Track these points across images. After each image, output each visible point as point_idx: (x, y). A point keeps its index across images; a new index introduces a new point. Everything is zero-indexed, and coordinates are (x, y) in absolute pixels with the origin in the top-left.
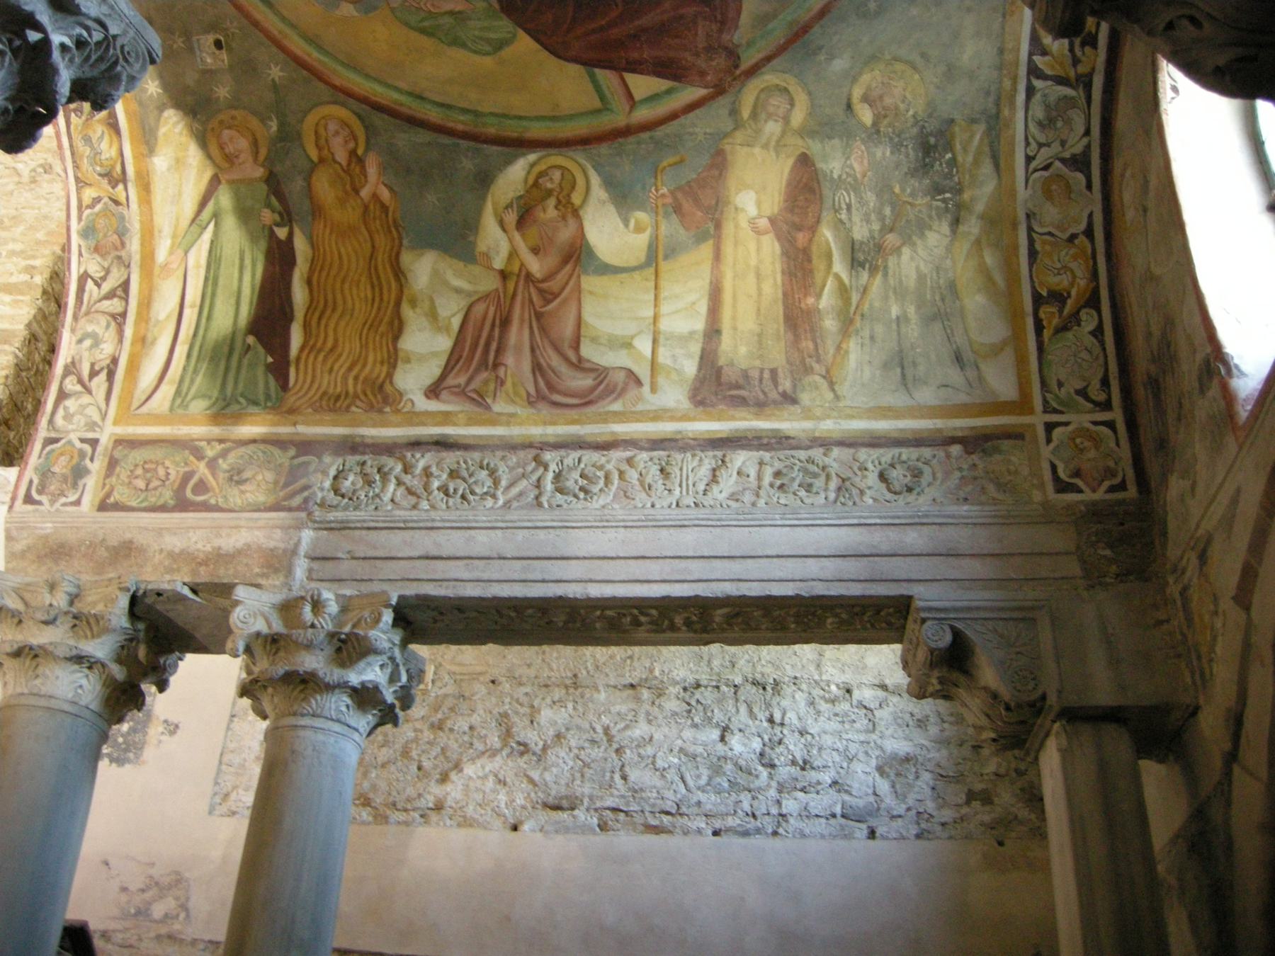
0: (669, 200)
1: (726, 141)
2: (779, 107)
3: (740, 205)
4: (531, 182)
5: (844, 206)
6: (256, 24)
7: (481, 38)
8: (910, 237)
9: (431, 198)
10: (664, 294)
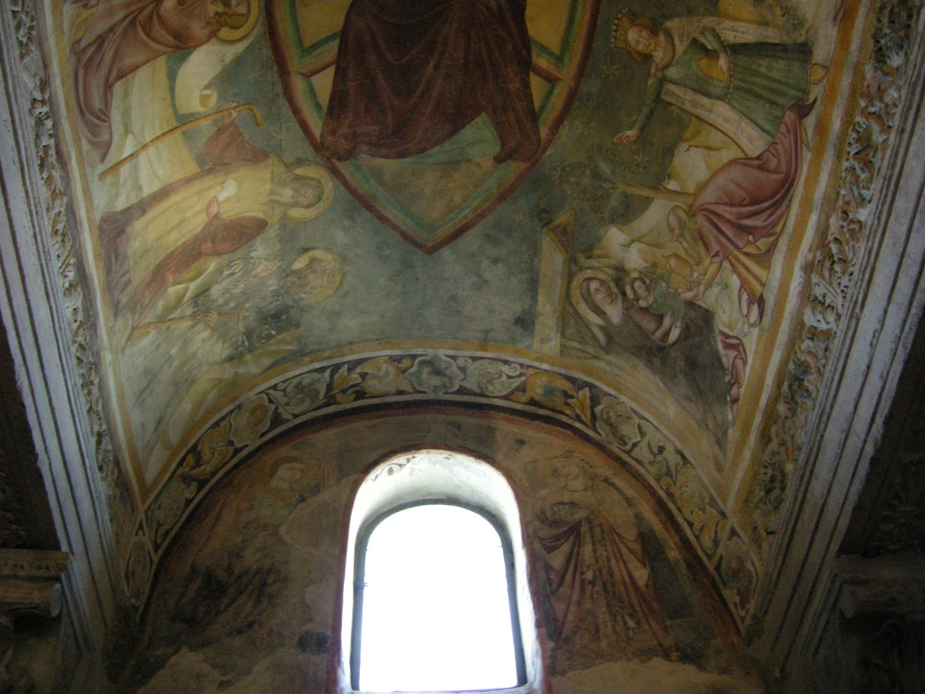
0: (227, 121)
1: (275, 159)
3: (226, 184)
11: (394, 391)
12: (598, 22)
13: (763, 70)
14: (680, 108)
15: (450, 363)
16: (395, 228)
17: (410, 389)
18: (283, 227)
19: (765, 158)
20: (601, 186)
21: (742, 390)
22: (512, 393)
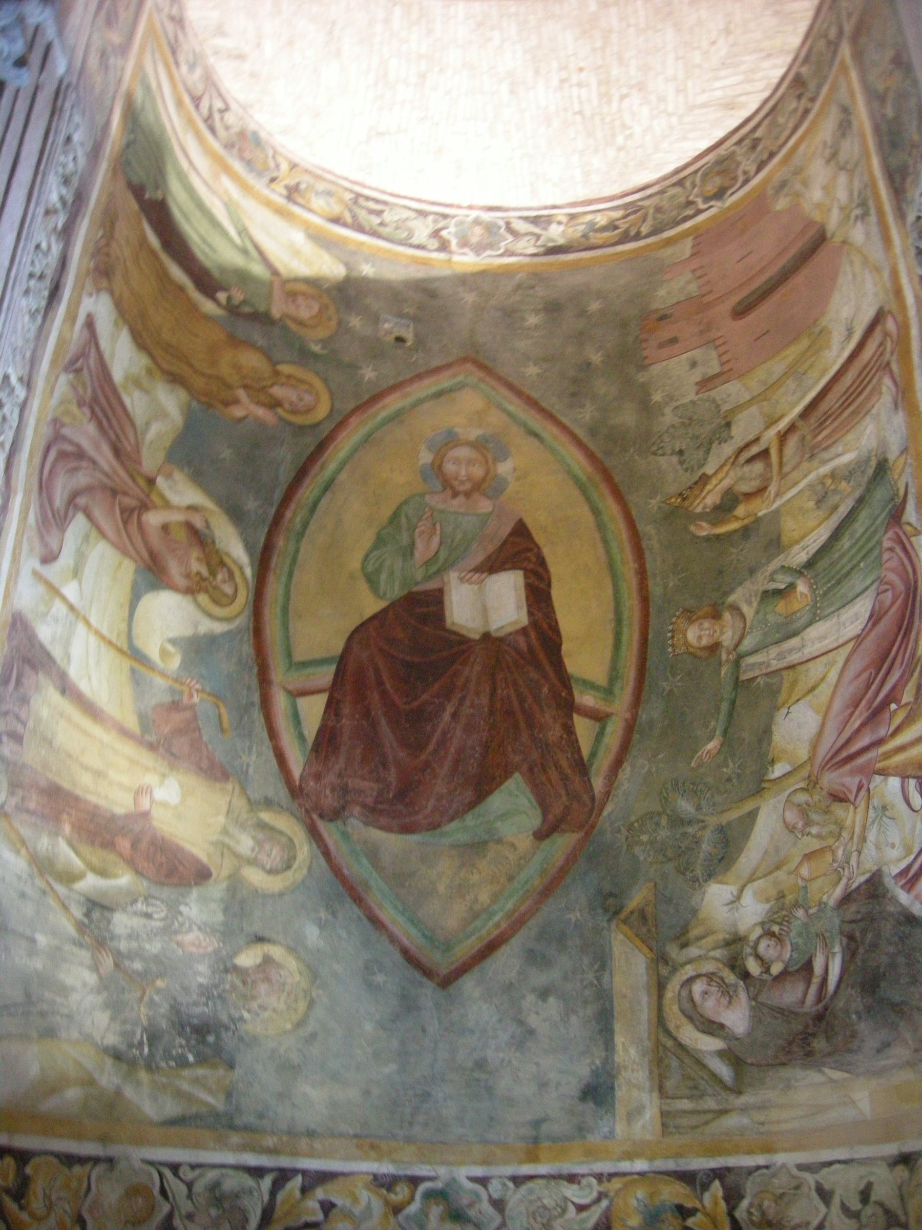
0: (185, 700)
2: (269, 856)
3: (166, 782)
4: (226, 560)
5: (150, 910)
6: (419, 377)
7: (381, 565)
8: (106, 988)
9: (226, 454)
10: (104, 648)
12: (650, 637)
14: (766, 674)
15: (477, 1195)
16: (393, 939)
20: (685, 835)
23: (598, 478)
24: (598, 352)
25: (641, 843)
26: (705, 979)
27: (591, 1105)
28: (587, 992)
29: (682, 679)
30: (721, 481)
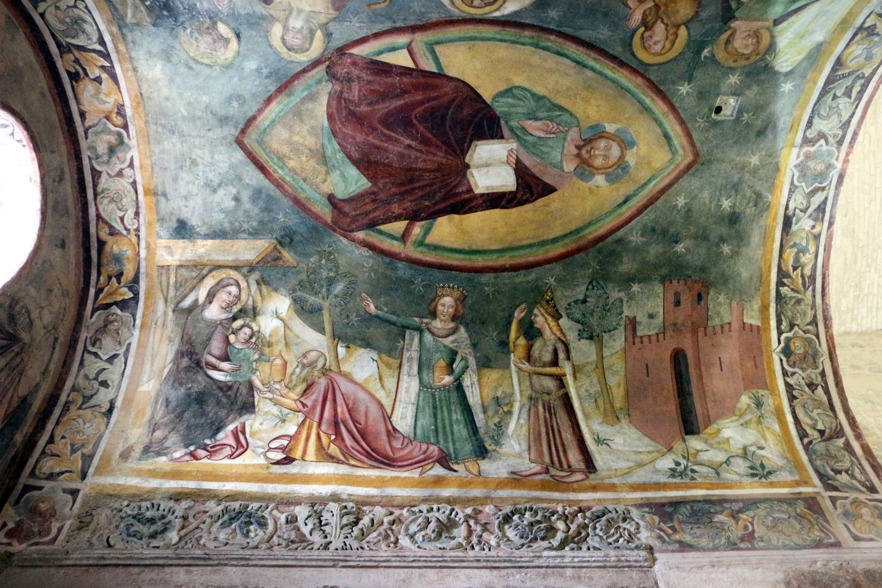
1: (333, 16)
6: (682, 122)
7: (520, 99)
11: (82, 108)
13: (454, 417)
15: (124, 161)
16: (260, 111)
17: (87, 124)
18: (263, 18)
19: (397, 435)
20: (322, 286)
21: (206, 461)
22: (106, 223)
23: (582, 242)
24: (685, 249)
25: (320, 260)
26: (237, 294)
27: (175, 225)
28: (237, 224)
29: (419, 290)
30: (550, 328)
